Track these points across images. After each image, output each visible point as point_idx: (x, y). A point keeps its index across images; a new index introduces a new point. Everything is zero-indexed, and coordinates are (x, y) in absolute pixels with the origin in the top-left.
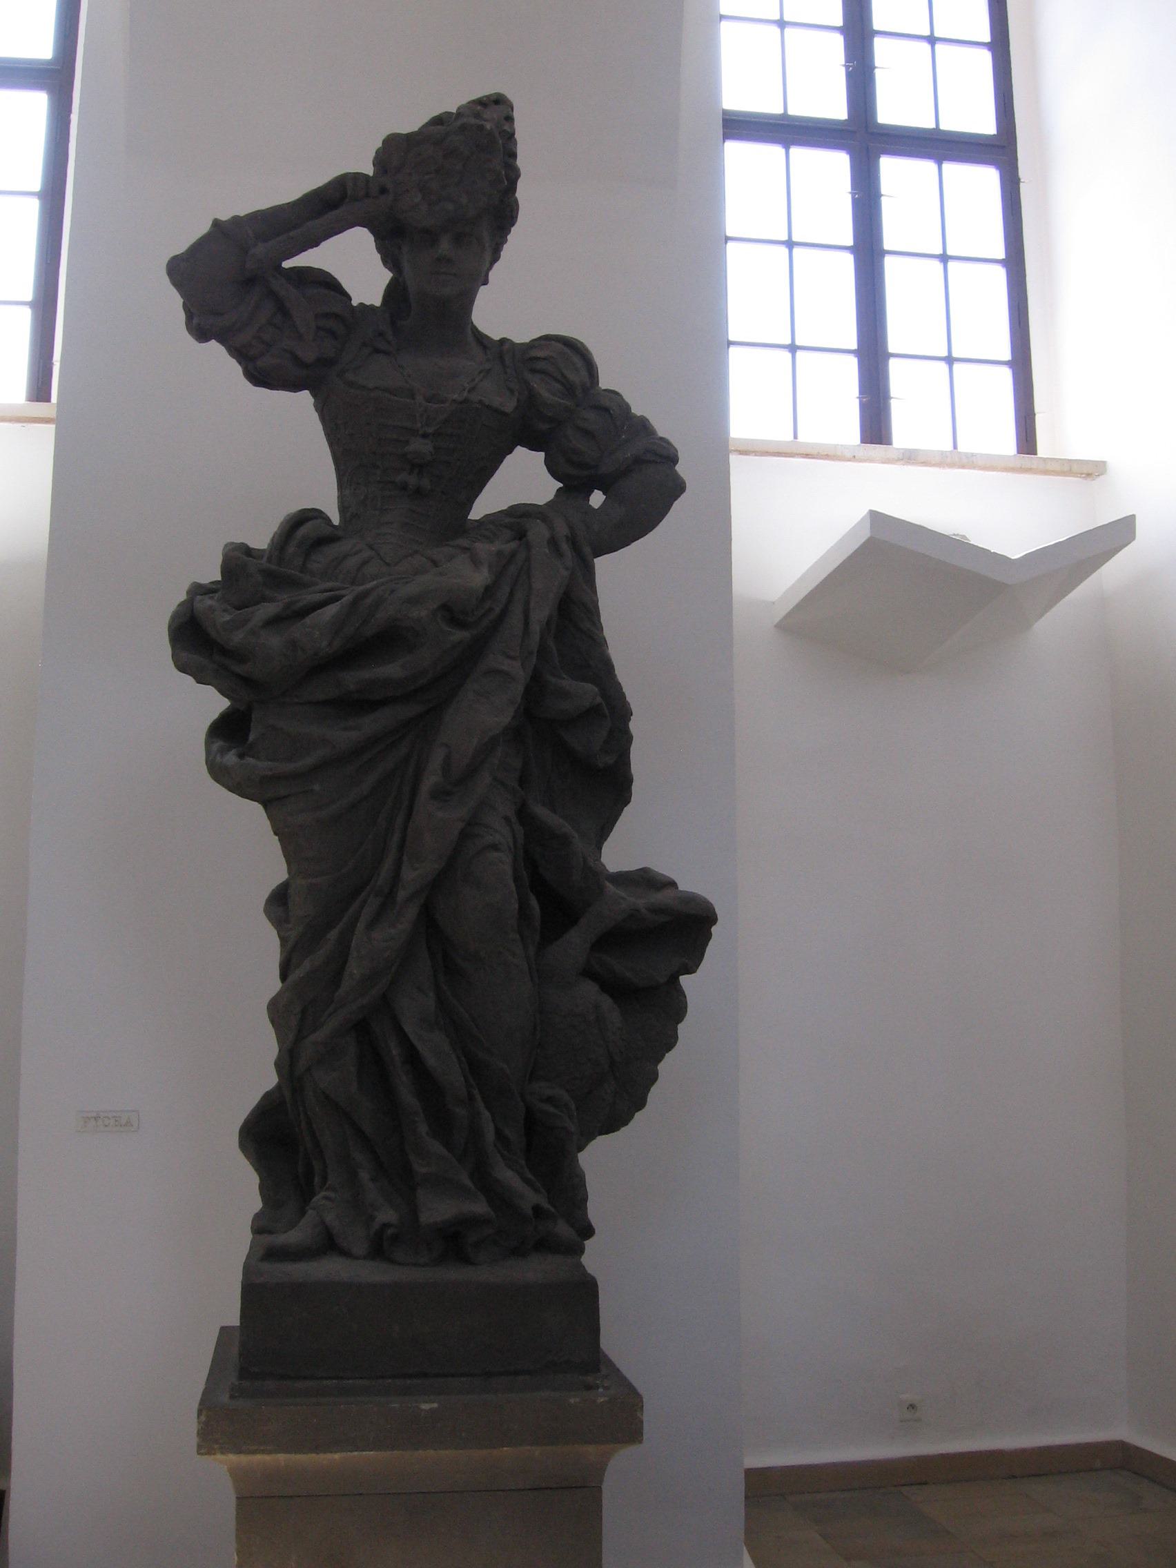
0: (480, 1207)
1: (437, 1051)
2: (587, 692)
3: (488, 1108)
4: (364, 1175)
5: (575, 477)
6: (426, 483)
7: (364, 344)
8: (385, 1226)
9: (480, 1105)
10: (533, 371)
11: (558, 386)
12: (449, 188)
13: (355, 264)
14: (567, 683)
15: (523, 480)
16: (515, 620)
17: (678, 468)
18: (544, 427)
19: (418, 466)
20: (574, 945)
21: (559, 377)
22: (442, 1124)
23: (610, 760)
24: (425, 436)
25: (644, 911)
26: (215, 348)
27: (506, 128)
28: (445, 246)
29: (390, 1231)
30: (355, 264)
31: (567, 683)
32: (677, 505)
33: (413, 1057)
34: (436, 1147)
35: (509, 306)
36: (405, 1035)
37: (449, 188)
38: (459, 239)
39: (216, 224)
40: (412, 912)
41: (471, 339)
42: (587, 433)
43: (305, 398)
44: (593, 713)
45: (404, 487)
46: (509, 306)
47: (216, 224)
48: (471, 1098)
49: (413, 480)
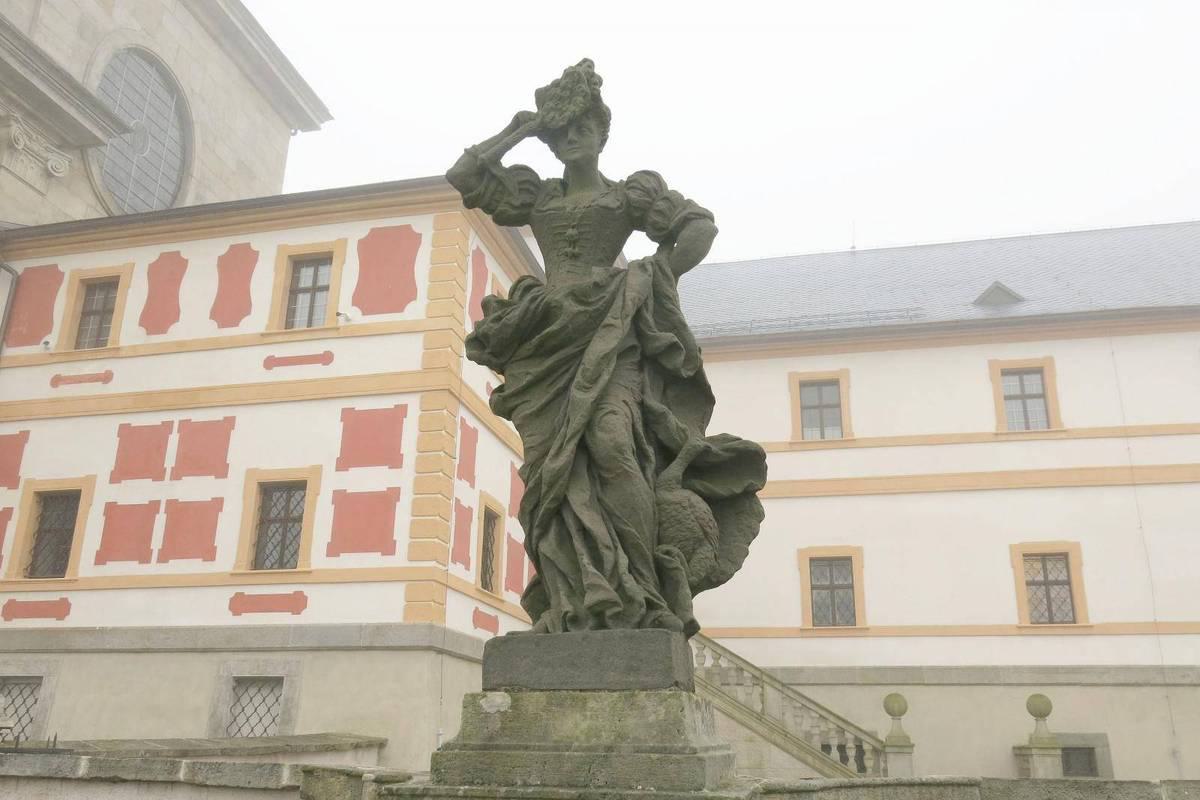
2: (670, 337)
5: (665, 237)
6: (577, 250)
7: (547, 195)
8: (566, 613)
9: (621, 551)
10: (629, 189)
11: (639, 192)
12: (573, 110)
14: (658, 334)
15: (639, 246)
16: (618, 302)
18: (637, 214)
19: (573, 242)
20: (676, 469)
21: (639, 186)
22: (598, 561)
23: (691, 374)
24: (573, 227)
25: (720, 452)
27: (590, 70)
28: (572, 135)
31: (658, 334)
32: (715, 240)
33: (585, 532)
34: (591, 569)
35: (615, 163)
37: (573, 110)
38: (580, 130)
40: (571, 447)
41: (601, 183)
42: (660, 212)
44: (673, 348)
45: (566, 254)
46: (615, 163)
47: (466, 150)
48: (616, 548)
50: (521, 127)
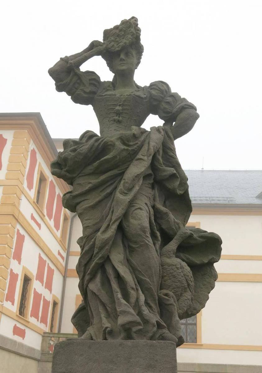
0: (138, 319)
1: (124, 271)
2: (172, 170)
3: (143, 293)
4: (103, 315)
5: (168, 118)
6: (121, 118)
7: (104, 89)
8: (107, 328)
9: (140, 292)
10: (151, 89)
11: (157, 91)
12: (122, 44)
13: (98, 66)
14: (164, 167)
15: (153, 122)
16: (145, 147)
17: (138, 26)
18: (155, 103)
19: (118, 114)
20: (173, 245)
21: (157, 88)
22: (126, 296)
23: (182, 192)
24: (120, 105)
25: (198, 238)
26: (64, 94)
27: (136, 23)
28: (122, 56)
29: (108, 329)
30: (98, 66)
31: (164, 167)
32: (197, 121)
33: (118, 277)
34: (123, 301)
36: (95, 241)
37: (122, 44)
38: (127, 54)
39: (61, 59)
40: (114, 227)
41: (134, 85)
42: (168, 103)
43: (90, 107)
44: (173, 177)
45: (114, 120)
47: (61, 59)
48: (137, 290)
49: (117, 118)
50: (94, 49)
